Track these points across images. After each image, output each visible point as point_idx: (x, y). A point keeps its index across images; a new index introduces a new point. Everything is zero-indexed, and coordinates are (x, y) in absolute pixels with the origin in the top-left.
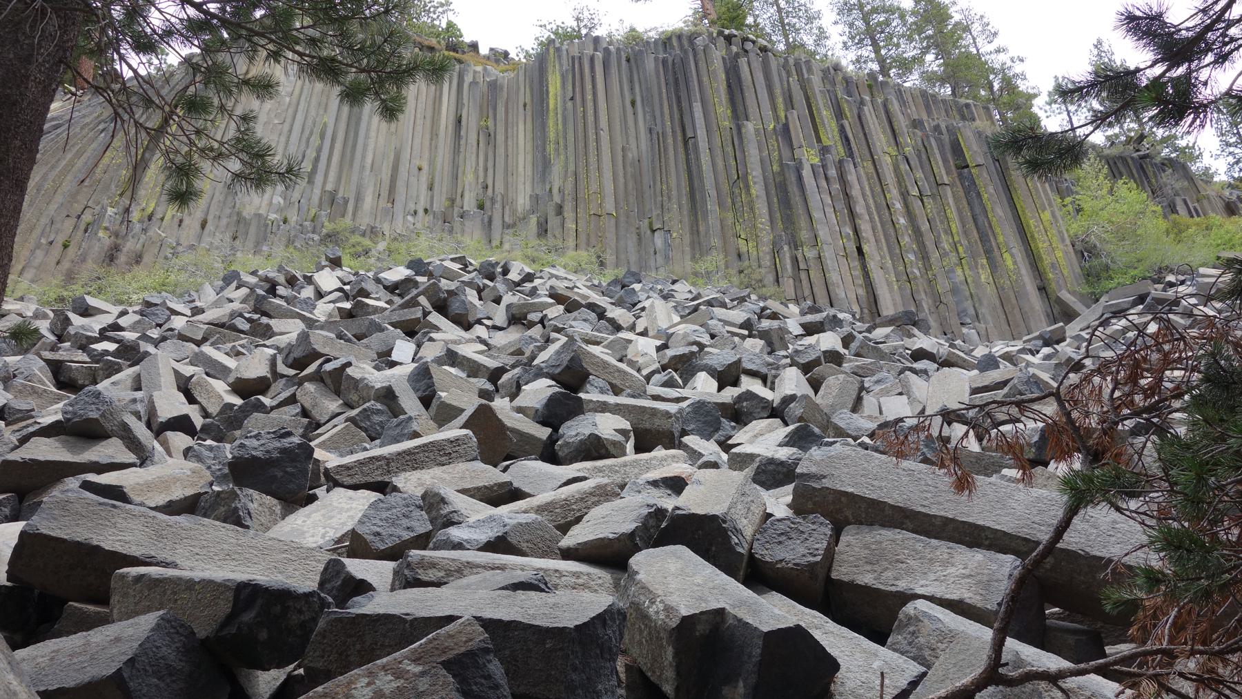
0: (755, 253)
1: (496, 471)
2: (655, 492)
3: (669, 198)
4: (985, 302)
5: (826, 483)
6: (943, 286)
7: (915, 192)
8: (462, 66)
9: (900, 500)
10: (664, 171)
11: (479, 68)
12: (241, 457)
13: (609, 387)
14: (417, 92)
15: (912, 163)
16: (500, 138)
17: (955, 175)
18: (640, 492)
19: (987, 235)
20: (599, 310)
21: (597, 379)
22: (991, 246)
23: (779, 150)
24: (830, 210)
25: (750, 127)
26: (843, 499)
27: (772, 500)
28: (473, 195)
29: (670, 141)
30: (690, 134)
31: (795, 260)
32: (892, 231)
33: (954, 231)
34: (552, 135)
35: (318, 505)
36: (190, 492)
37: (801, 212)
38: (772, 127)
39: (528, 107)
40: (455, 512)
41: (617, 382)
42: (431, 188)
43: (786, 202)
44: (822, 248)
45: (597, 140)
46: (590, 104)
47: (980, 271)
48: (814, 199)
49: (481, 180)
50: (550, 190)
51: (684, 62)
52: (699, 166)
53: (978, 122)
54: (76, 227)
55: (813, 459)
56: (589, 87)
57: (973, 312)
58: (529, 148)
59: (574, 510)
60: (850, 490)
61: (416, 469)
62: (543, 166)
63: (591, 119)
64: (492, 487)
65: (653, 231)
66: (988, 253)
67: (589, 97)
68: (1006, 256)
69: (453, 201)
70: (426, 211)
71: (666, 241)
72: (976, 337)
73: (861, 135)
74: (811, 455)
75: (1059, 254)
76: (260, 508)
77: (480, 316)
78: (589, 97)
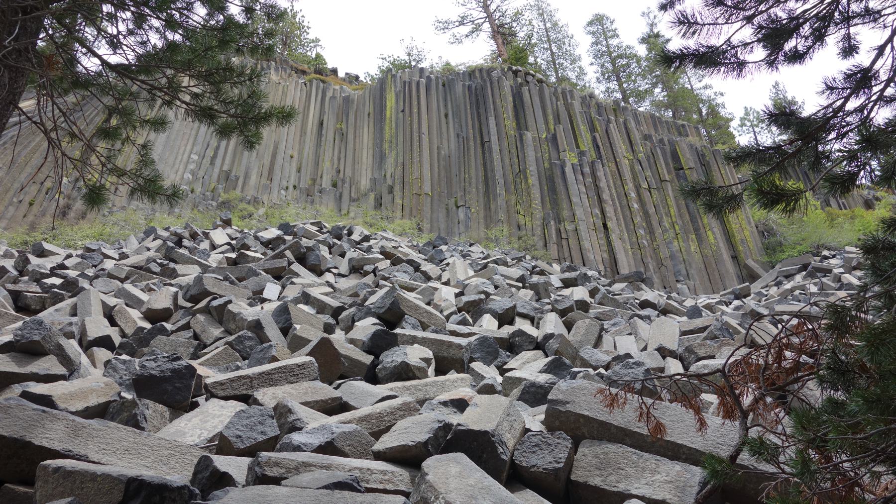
0: (530, 225)
1: (331, 388)
2: (445, 410)
3: (470, 184)
4: (694, 266)
5: (569, 407)
6: (664, 253)
7: (645, 185)
8: (325, 85)
9: (622, 422)
10: (466, 164)
11: (337, 87)
12: (142, 375)
13: (419, 324)
14: (268, 132)
15: (643, 165)
16: (351, 137)
17: (674, 174)
18: (433, 410)
20: (415, 265)
21: (410, 318)
22: (699, 226)
23: (549, 153)
24: (584, 196)
25: (529, 136)
26: (581, 420)
27: (531, 418)
28: (329, 176)
29: (472, 143)
30: (486, 139)
31: (559, 232)
32: (628, 213)
33: (673, 214)
34: (387, 136)
35: (197, 412)
36: (102, 400)
37: (563, 197)
38: (544, 136)
40: (298, 419)
41: (425, 320)
42: (299, 171)
43: (553, 190)
44: (578, 223)
45: (420, 141)
46: (415, 116)
47: (691, 243)
48: (573, 188)
49: (336, 166)
50: (385, 175)
51: (483, 88)
52: (492, 162)
53: (690, 138)
54: (39, 191)
55: (562, 388)
56: (415, 103)
57: (685, 273)
58: (371, 145)
59: (385, 421)
60: (586, 413)
61: (272, 385)
62: (380, 158)
63: (415, 126)
64: (327, 400)
65: (458, 207)
66: (697, 230)
67: (415, 110)
68: (709, 233)
69: (314, 181)
70: (295, 187)
71: (466, 214)
72: (687, 291)
73: (608, 144)
74: (559, 386)
75: (747, 233)
76: (154, 414)
77: (329, 266)
78: (415, 110)
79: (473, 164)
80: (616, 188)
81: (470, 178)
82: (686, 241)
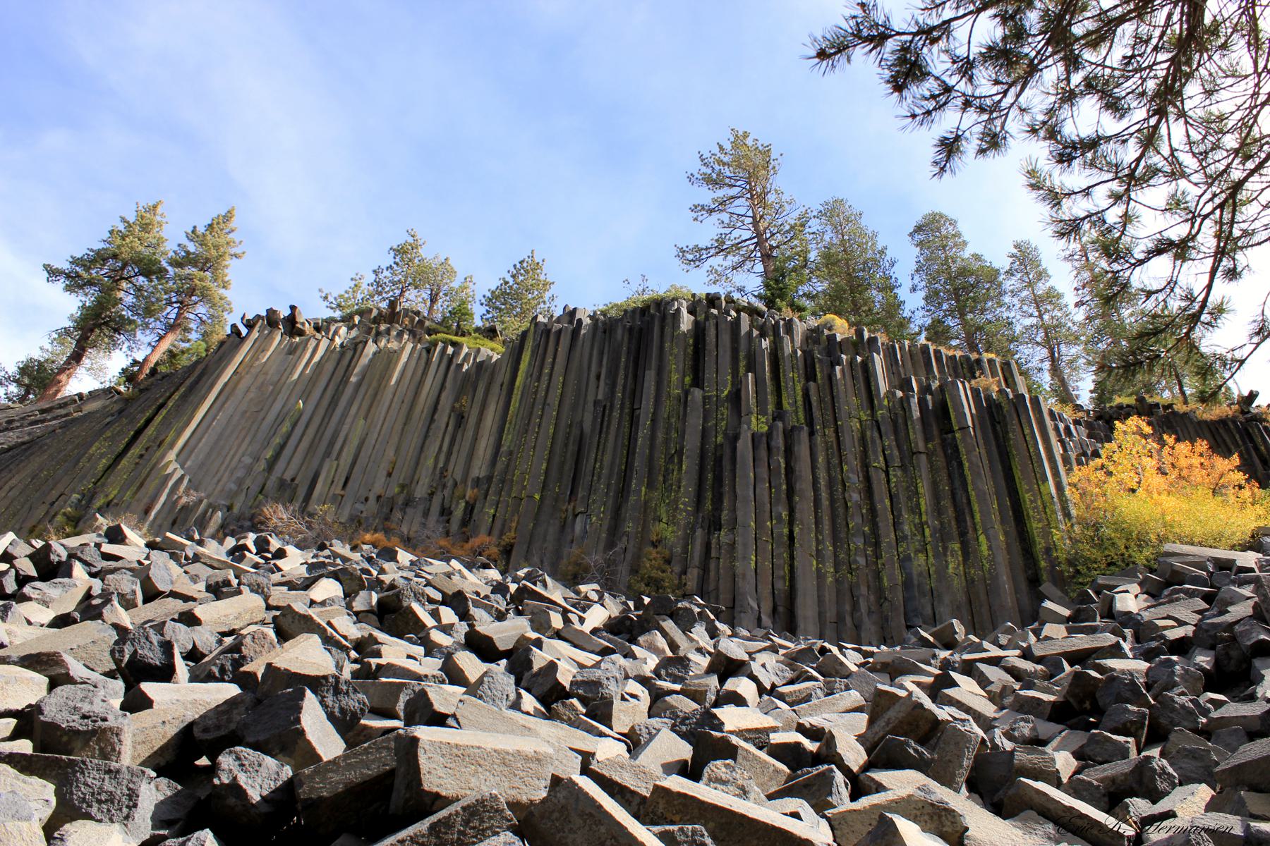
3: (599, 478)
4: (947, 599)
6: (892, 577)
10: (601, 447)
15: (883, 428)
16: (472, 421)
17: (937, 441)
19: (964, 513)
22: (966, 527)
29: (616, 414)
32: (841, 510)
33: (923, 509)
37: (727, 489)
39: (504, 386)
42: (389, 475)
43: (718, 480)
47: (949, 559)
49: (441, 465)
66: (963, 534)
68: (982, 538)
73: (828, 399)
79: (610, 445)
80: (828, 470)
81: (601, 468)
82: (942, 555)
